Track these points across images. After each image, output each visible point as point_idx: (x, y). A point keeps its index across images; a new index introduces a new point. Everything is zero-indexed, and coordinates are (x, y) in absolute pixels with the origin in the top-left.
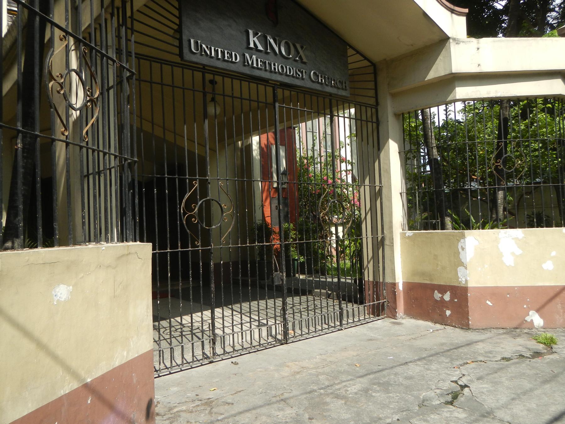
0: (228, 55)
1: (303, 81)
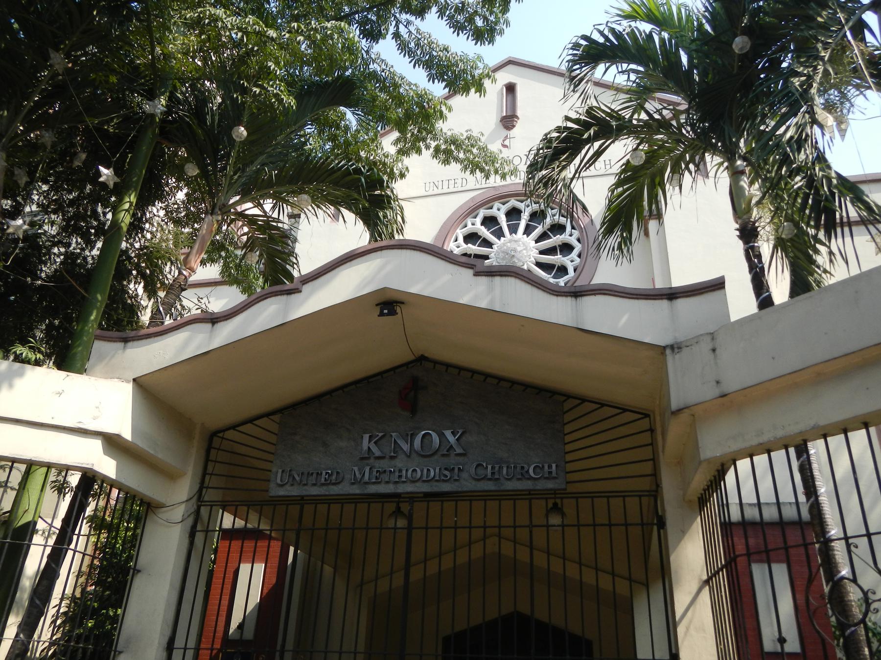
0: (327, 476)
1: (457, 483)
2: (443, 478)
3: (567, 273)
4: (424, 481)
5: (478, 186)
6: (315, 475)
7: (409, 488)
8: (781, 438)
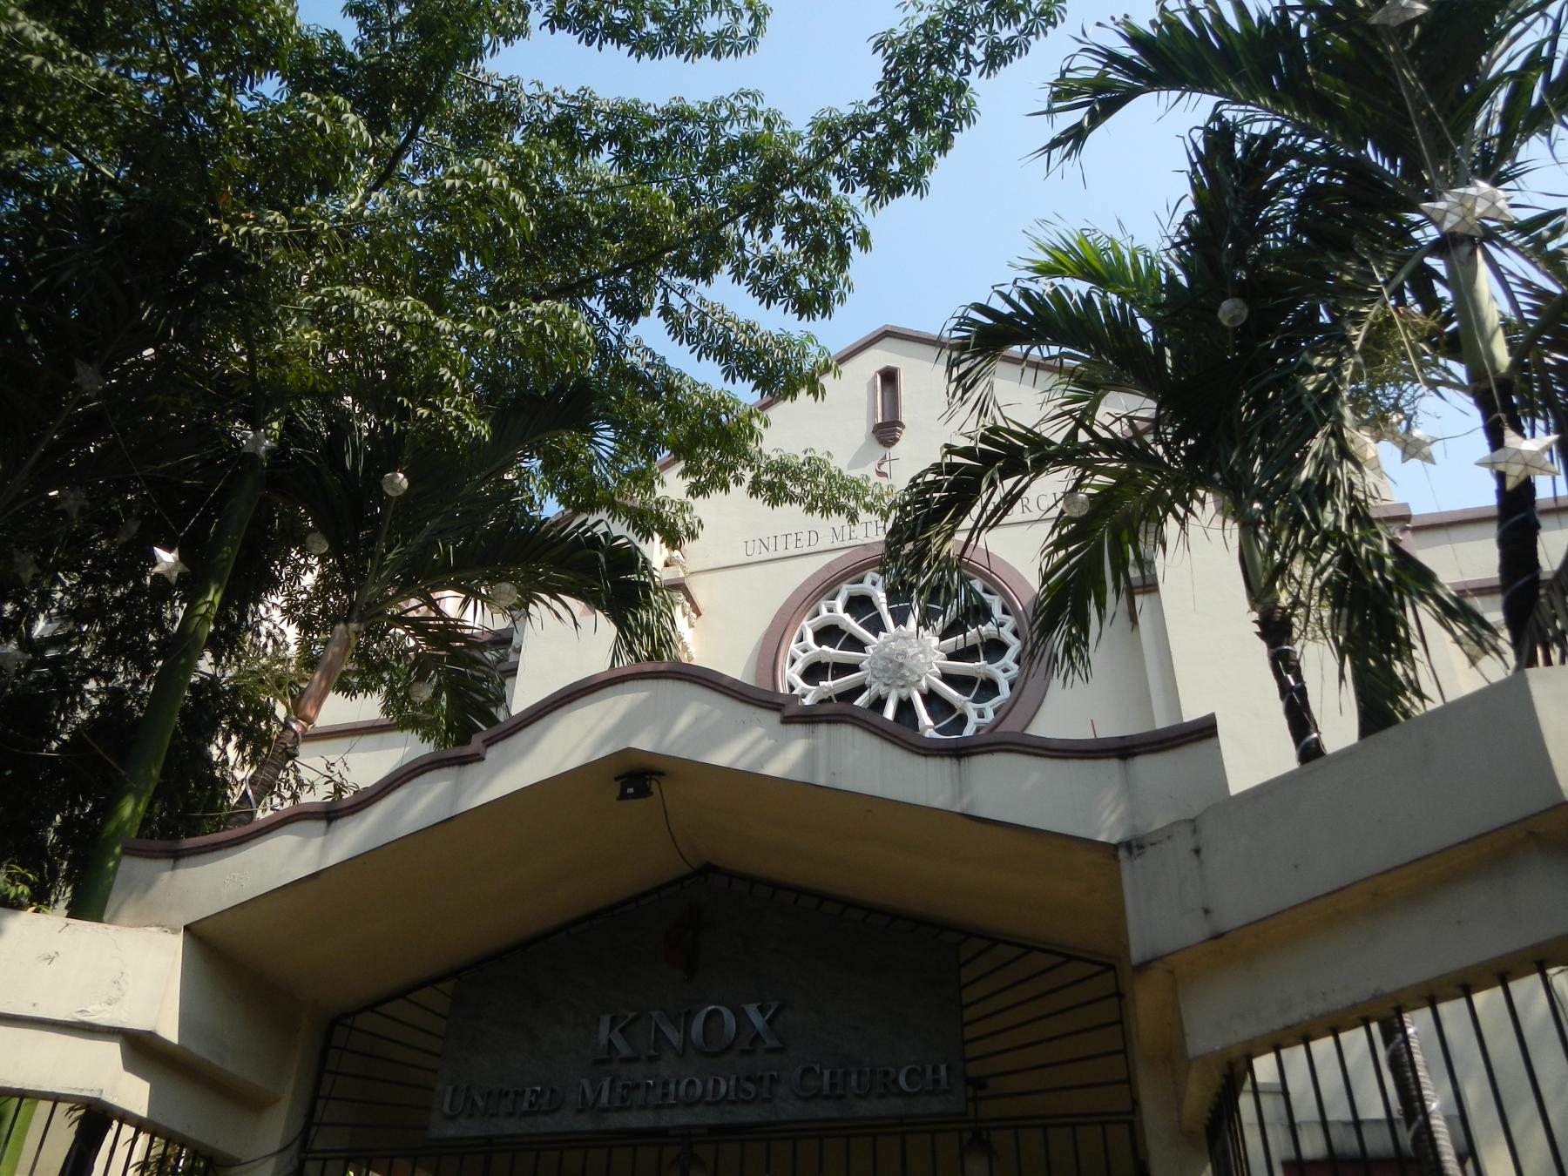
0: (533, 1099)
2: (742, 1096)
3: (998, 694)
4: (709, 1104)
5: (837, 544)
6: (511, 1096)
7: (683, 1118)
8: (1321, 1016)
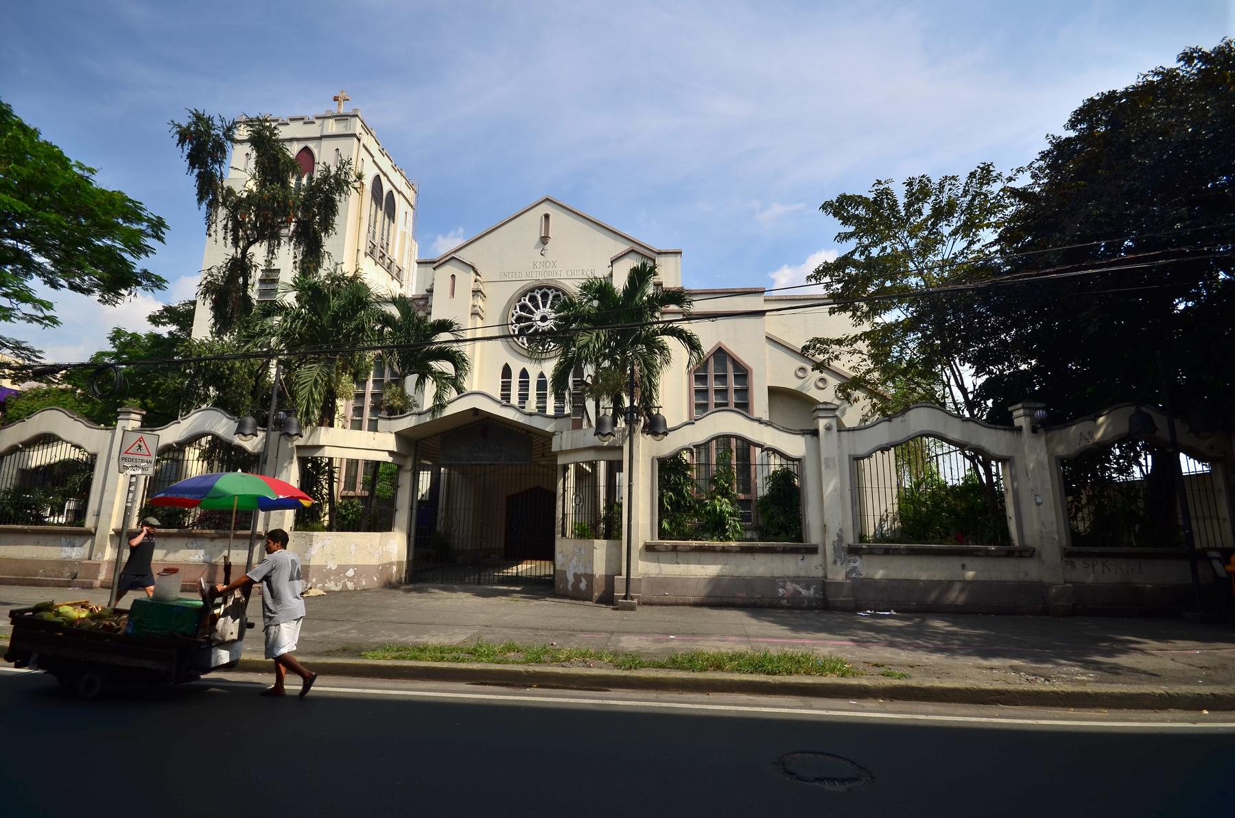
7: (485, 462)
